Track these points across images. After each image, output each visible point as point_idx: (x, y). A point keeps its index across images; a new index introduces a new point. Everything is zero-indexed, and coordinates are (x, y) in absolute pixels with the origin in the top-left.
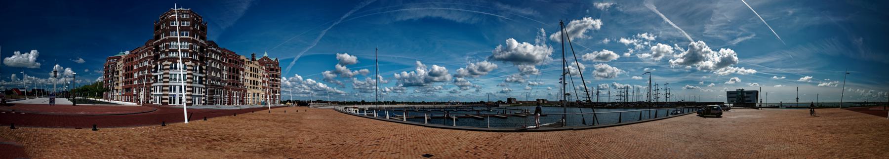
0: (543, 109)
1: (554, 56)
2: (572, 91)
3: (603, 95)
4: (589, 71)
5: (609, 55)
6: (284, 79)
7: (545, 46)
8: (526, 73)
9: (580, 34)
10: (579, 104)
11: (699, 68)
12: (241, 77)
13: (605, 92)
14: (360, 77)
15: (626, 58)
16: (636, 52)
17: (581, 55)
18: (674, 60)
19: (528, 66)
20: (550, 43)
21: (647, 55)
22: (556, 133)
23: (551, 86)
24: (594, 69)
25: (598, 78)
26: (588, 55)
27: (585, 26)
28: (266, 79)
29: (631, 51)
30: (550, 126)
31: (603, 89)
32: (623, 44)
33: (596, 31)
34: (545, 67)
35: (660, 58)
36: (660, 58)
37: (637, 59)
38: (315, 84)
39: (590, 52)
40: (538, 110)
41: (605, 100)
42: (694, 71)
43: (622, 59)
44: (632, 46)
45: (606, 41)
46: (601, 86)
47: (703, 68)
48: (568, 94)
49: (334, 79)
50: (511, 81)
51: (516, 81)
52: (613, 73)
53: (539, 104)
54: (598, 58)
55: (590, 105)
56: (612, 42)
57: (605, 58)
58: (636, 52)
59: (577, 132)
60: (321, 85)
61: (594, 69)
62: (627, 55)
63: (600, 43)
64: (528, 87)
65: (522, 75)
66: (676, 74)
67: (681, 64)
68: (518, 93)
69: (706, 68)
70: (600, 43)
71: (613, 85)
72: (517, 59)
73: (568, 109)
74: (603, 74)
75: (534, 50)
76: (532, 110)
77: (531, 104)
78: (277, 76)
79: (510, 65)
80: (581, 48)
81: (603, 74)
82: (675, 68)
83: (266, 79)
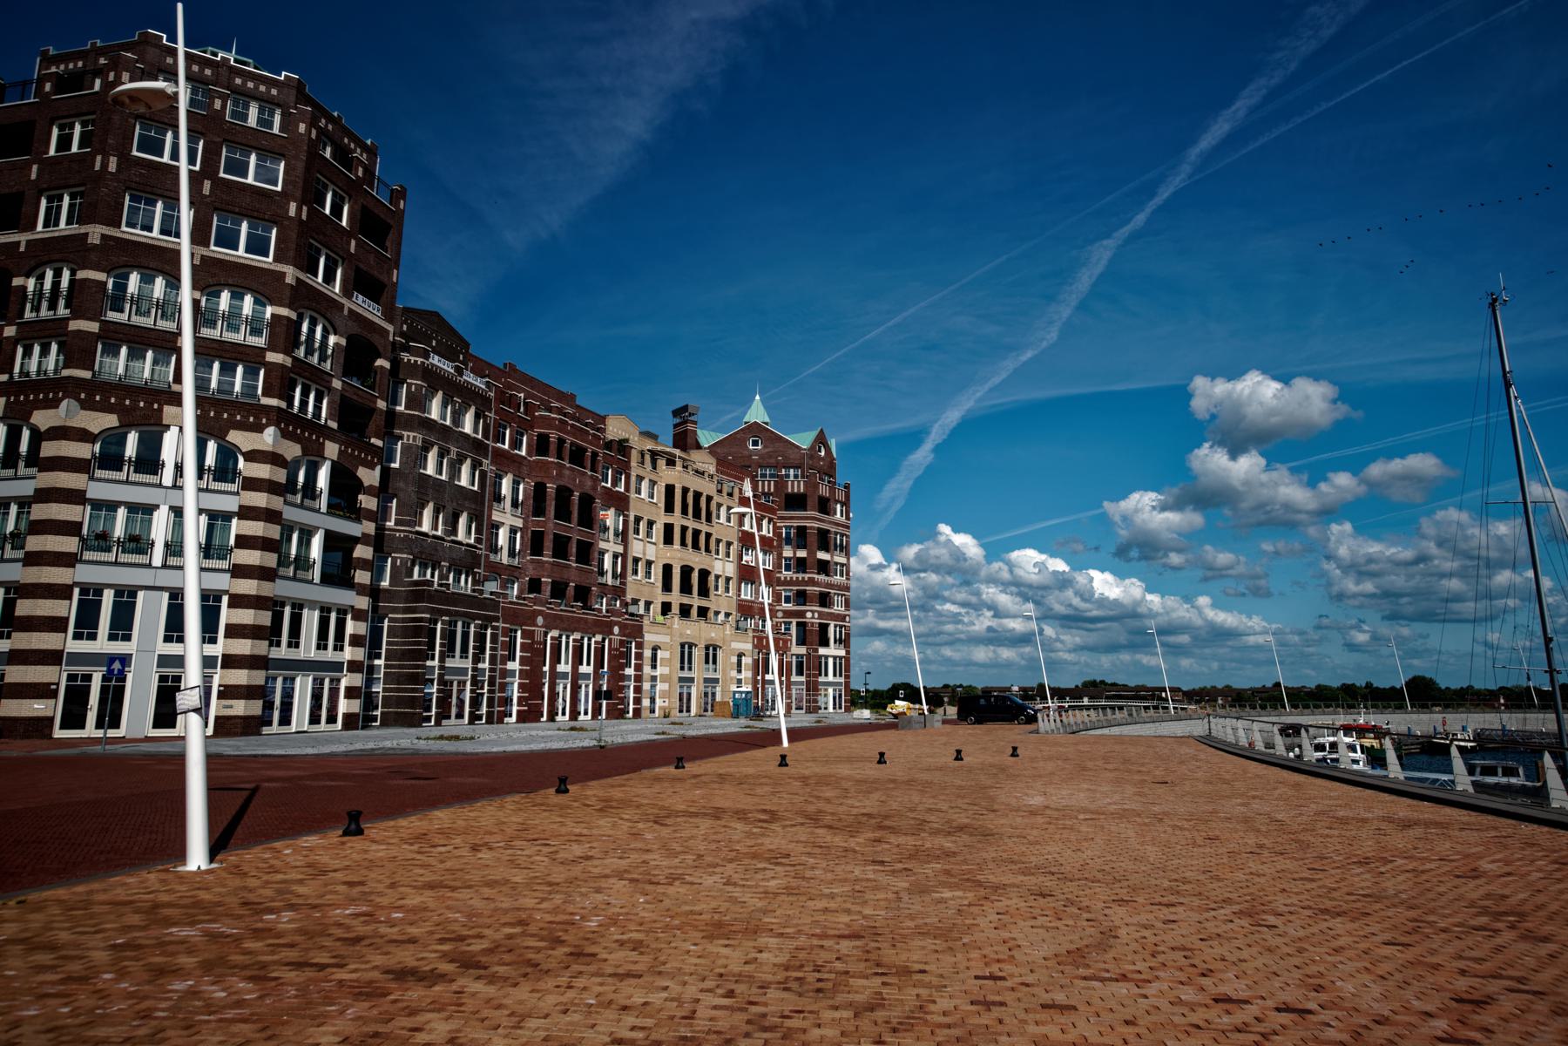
6: (872, 553)
12: (610, 546)
14: (1370, 512)
28: (759, 559)
38: (1063, 582)
49: (1188, 540)
60: (1104, 584)
78: (824, 540)
83: (759, 559)
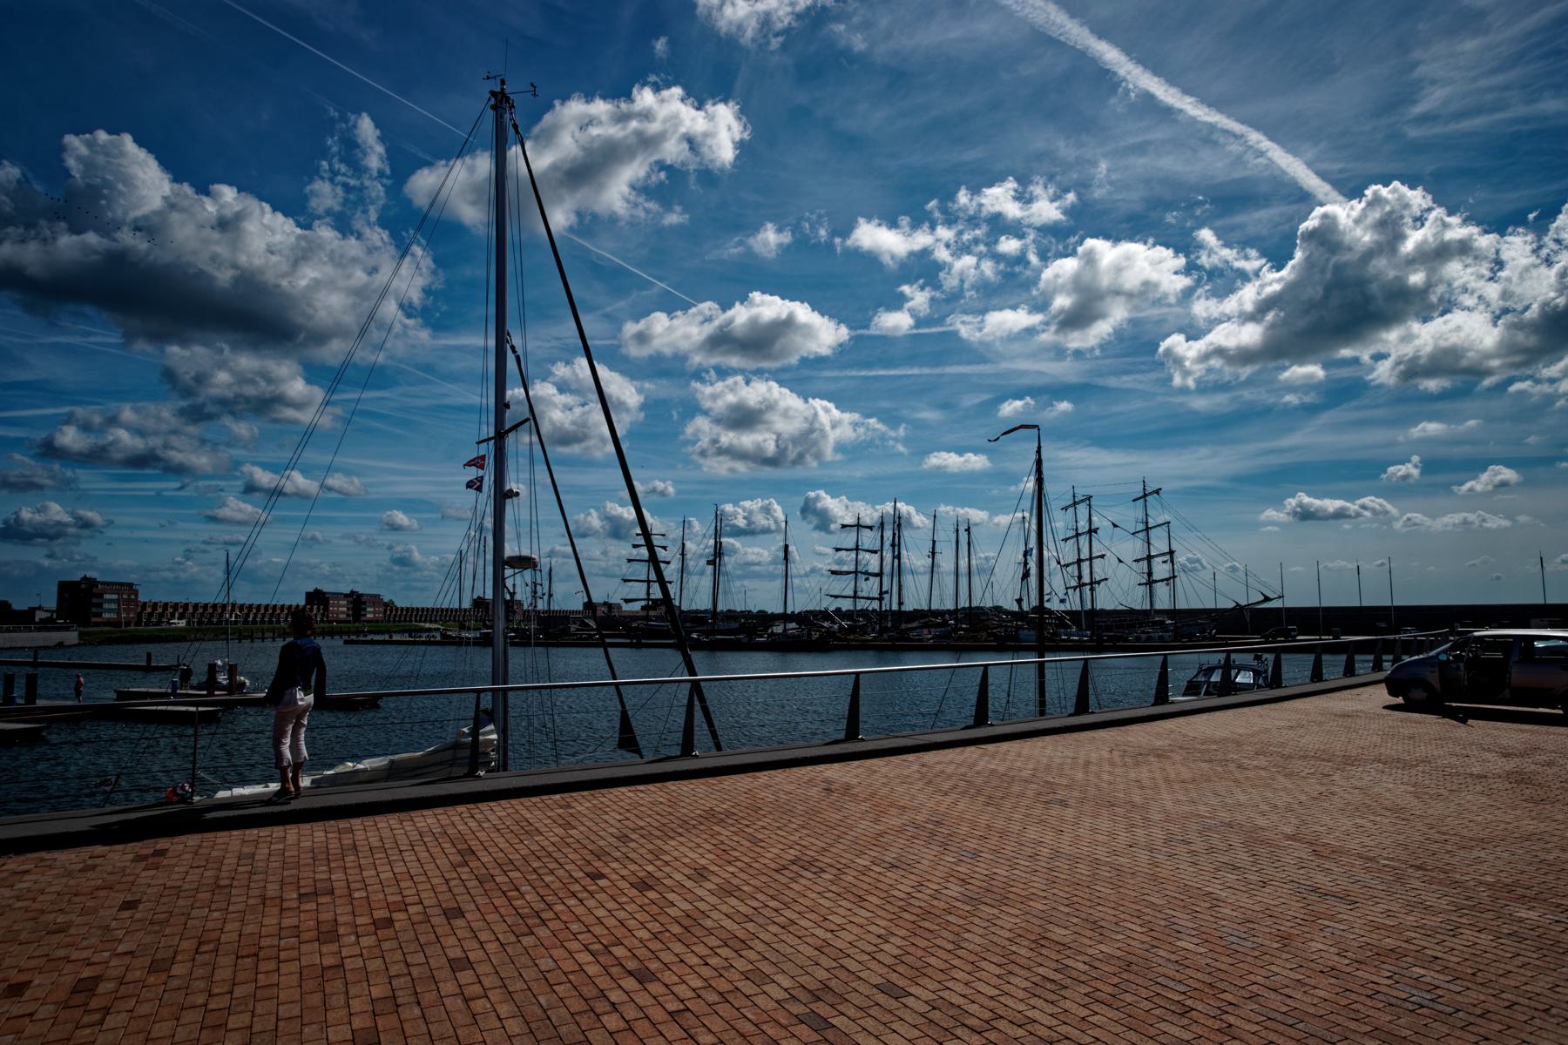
0: (337, 656)
1: (435, 312)
2: (548, 545)
3: (749, 570)
4: (666, 419)
5: (788, 324)
7: (378, 236)
8: (231, 406)
9: (616, 193)
10: (603, 626)
11: (1384, 373)
13: (760, 552)
15: (886, 340)
16: (950, 301)
17: (616, 321)
18: (1193, 334)
19: (247, 362)
20: (414, 225)
21: (1010, 319)
22: (427, 819)
23: (408, 505)
24: (693, 409)
25: (721, 467)
26: (659, 322)
27: (647, 142)
29: (919, 298)
30: (394, 772)
31: (749, 532)
32: (870, 259)
33: (708, 176)
34: (375, 377)
35: (1102, 329)
36: (1102, 329)
37: (950, 348)
39: (672, 306)
40: (300, 666)
41: (762, 597)
42: (1345, 391)
43: (865, 350)
44: (923, 268)
45: (770, 238)
46: (738, 513)
47: (1413, 370)
48: (524, 563)
50: (96, 457)
51: (141, 461)
52: (808, 438)
53: (308, 630)
54: (722, 340)
55: (667, 626)
56: (802, 245)
57: (760, 343)
58: (950, 301)
59: (582, 802)
61: (693, 409)
62: (897, 321)
63: (732, 250)
64: (237, 507)
65: (197, 414)
66: (1213, 427)
67: (1244, 356)
68: (159, 549)
69: (1445, 361)
70: (732, 250)
71: (808, 509)
72: (157, 299)
73: (518, 659)
74: (747, 440)
75: (302, 255)
76: (259, 662)
77: (253, 623)
79: (99, 335)
80: (614, 279)
81: (747, 440)
82: (1203, 388)
